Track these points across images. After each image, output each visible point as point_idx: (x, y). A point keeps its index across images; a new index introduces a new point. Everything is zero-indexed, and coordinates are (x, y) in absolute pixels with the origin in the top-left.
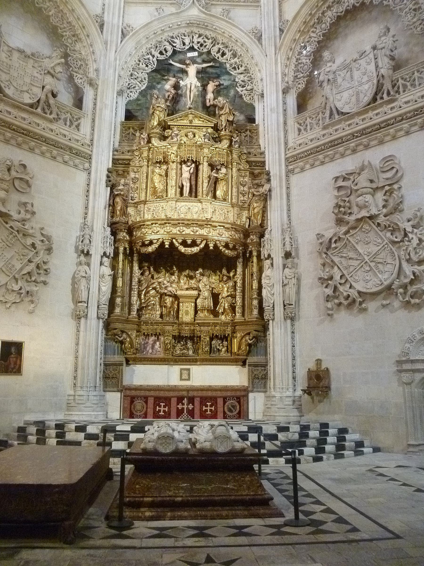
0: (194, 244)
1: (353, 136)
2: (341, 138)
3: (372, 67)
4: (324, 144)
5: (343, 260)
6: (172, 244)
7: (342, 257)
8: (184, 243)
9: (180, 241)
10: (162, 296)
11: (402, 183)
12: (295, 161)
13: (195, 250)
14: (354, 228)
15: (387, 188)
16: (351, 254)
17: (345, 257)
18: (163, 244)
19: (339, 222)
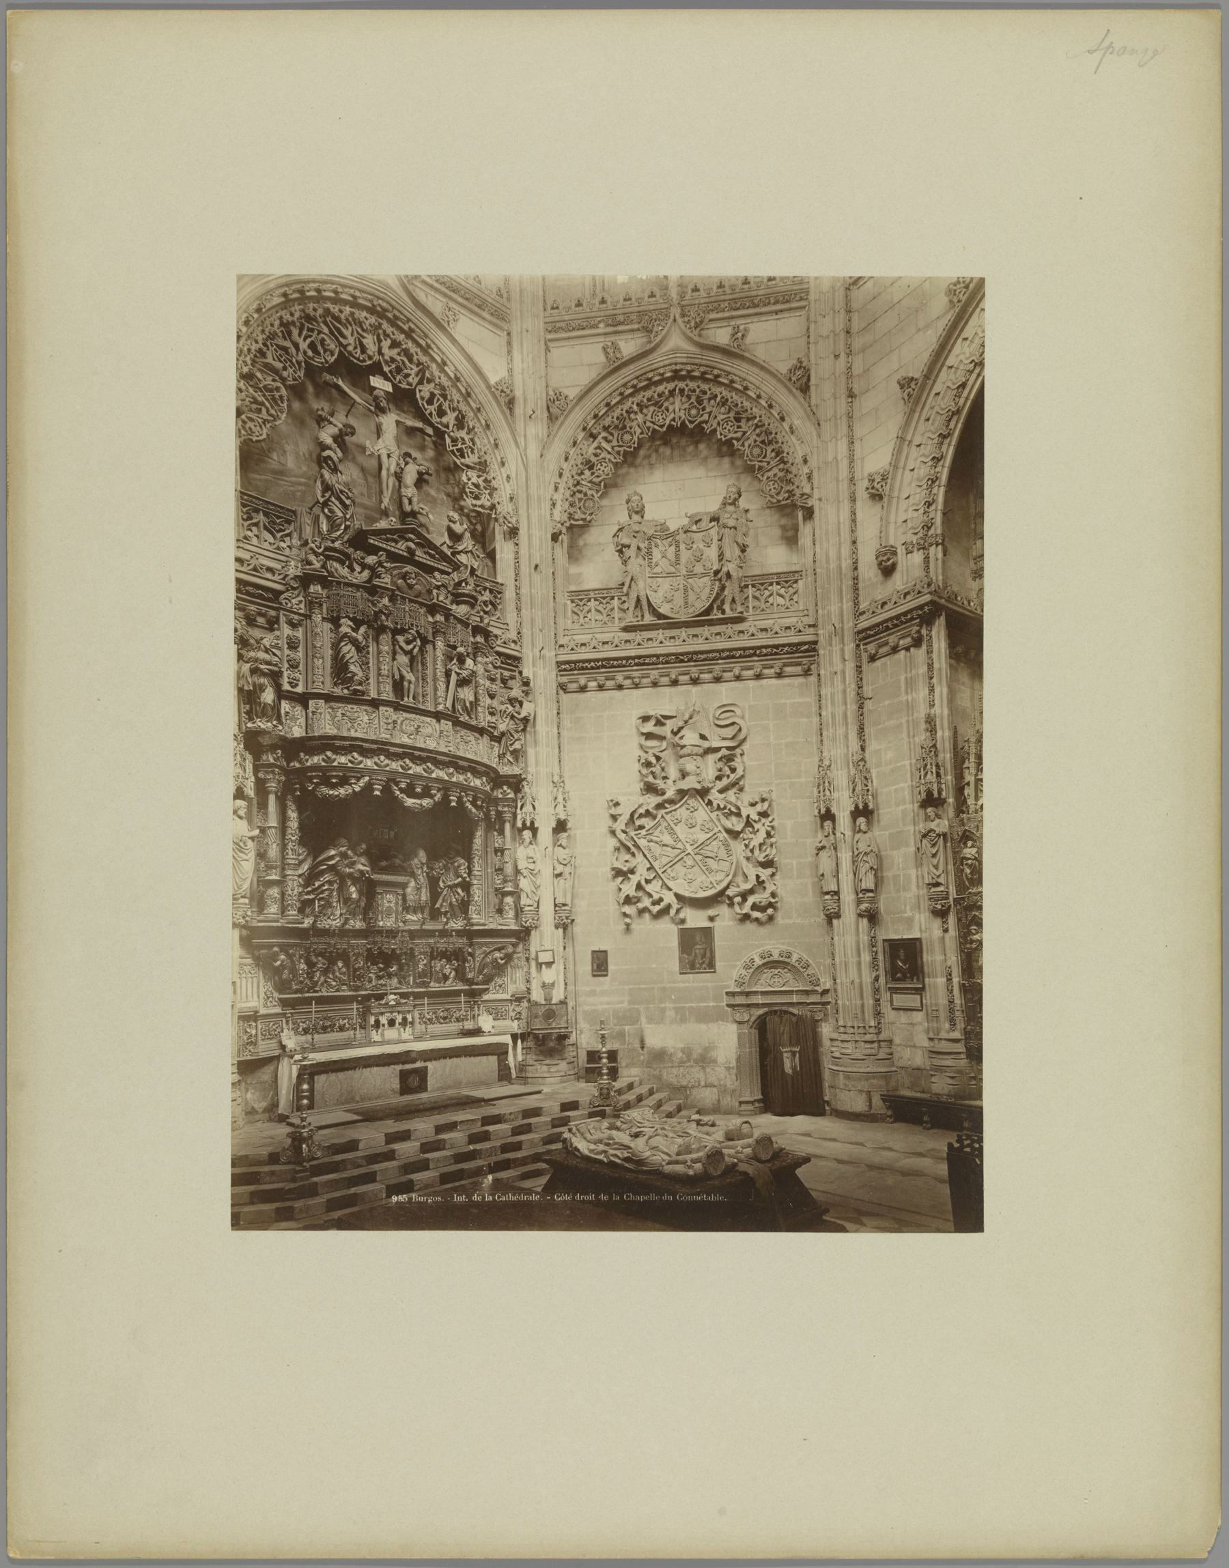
0: (426, 793)
1: (679, 658)
2: (657, 656)
3: (712, 553)
4: (627, 658)
5: (652, 844)
6: (387, 790)
7: (651, 841)
8: (409, 791)
9: (403, 786)
10: (343, 878)
11: (746, 747)
12: (571, 670)
13: (426, 802)
14: (671, 802)
15: (724, 752)
16: (667, 839)
17: (656, 843)
18: (369, 787)
19: (650, 789)
